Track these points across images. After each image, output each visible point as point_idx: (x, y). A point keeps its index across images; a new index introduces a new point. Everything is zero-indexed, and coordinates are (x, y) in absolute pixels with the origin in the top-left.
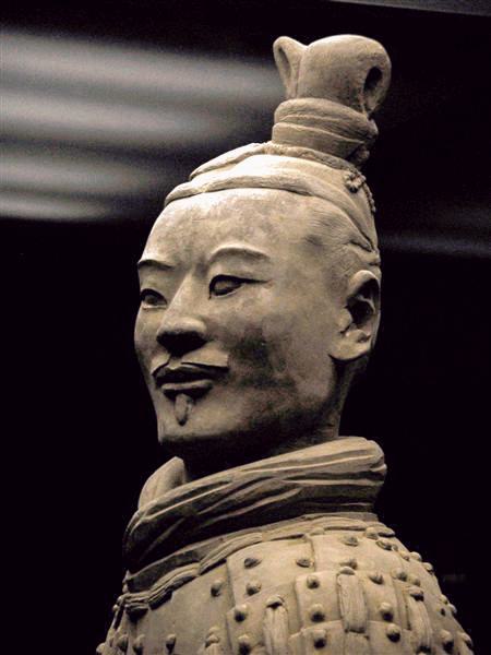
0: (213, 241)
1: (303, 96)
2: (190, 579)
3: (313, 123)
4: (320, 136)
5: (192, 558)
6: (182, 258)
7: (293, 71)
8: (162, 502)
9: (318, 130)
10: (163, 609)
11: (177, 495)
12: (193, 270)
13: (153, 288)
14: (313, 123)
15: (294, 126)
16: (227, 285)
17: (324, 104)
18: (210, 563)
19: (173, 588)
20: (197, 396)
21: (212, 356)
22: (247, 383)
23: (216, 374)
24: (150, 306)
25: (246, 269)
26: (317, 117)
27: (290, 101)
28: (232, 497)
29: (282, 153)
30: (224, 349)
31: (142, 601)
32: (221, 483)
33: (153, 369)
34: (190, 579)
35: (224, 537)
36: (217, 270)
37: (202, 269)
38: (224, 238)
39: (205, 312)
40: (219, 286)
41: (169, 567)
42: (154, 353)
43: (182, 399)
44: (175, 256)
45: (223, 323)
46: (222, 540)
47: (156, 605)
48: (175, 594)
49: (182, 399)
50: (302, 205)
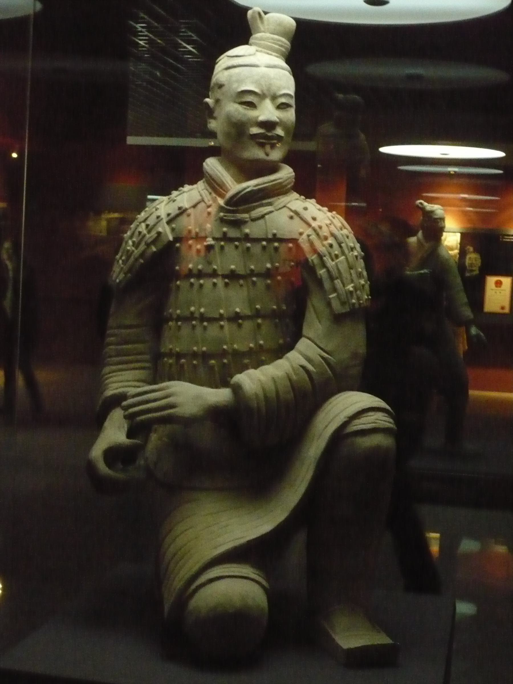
0: (279, 88)
1: (274, 34)
2: (271, 212)
3: (281, 46)
4: (283, 51)
5: (270, 204)
6: (265, 92)
7: (266, 23)
8: (260, 183)
9: (283, 50)
10: (261, 222)
11: (266, 181)
12: (269, 98)
13: (253, 101)
14: (281, 46)
15: (274, 45)
16: (285, 106)
17: (283, 40)
18: (280, 206)
19: (266, 214)
21: (279, 131)
23: (279, 138)
24: (248, 108)
26: (283, 44)
27: (263, 34)
28: (284, 184)
29: (271, 55)
30: (283, 130)
31: (247, 218)
32: (280, 179)
33: (251, 133)
34: (271, 212)
35: (279, 197)
36: (283, 100)
37: (274, 98)
38: (284, 88)
39: (278, 116)
40: (281, 107)
41: (262, 205)
42: (252, 126)
43: (268, 148)
44: (262, 91)
45: (285, 120)
46: (279, 199)
47: (254, 220)
48: (267, 217)
49: (268, 148)
50: (224, 66)
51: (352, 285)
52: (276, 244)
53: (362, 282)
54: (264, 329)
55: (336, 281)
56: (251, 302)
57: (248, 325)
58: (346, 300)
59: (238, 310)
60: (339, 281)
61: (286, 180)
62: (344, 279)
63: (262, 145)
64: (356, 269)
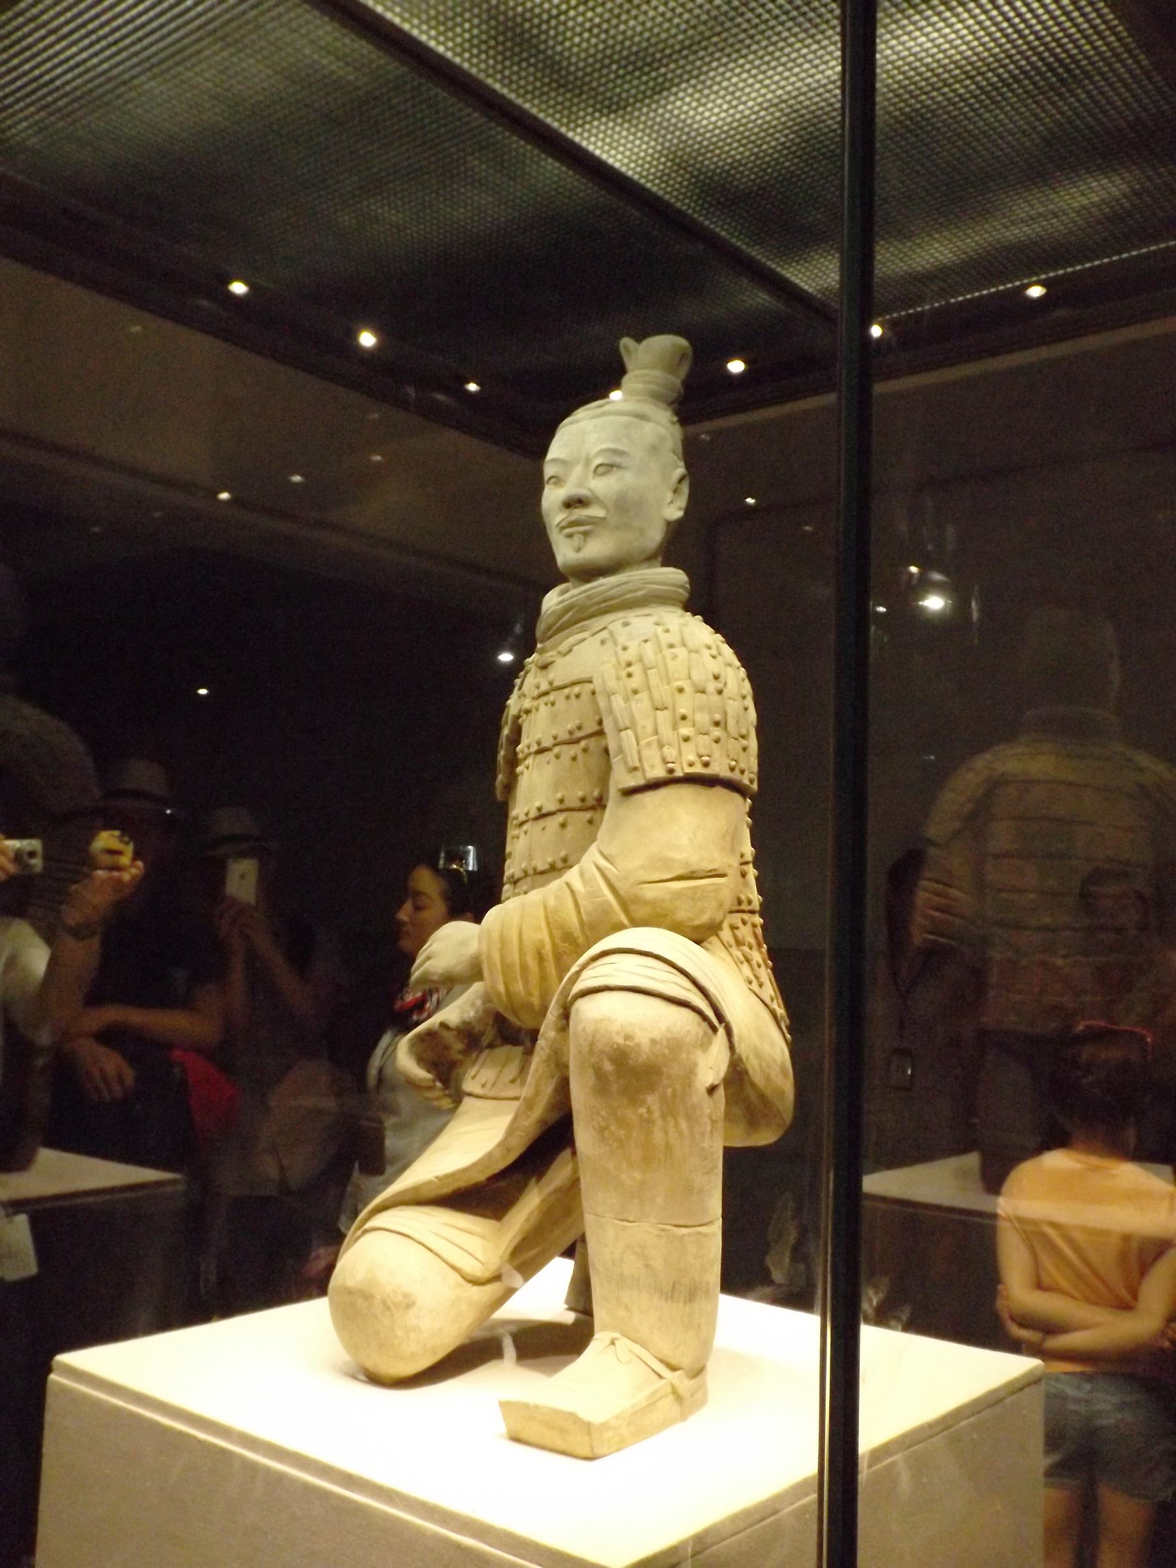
5: (582, 630)
9: (653, 387)
10: (568, 658)
20: (586, 534)
21: (595, 512)
22: (617, 528)
25: (617, 460)
36: (599, 461)
51: (655, 737)
52: (576, 689)
53: (685, 731)
54: (570, 831)
55: (623, 734)
56: (556, 786)
57: (553, 823)
58: (637, 764)
59: (537, 804)
60: (629, 732)
61: (617, 586)
62: (639, 727)
63: (570, 536)
64: (674, 710)
